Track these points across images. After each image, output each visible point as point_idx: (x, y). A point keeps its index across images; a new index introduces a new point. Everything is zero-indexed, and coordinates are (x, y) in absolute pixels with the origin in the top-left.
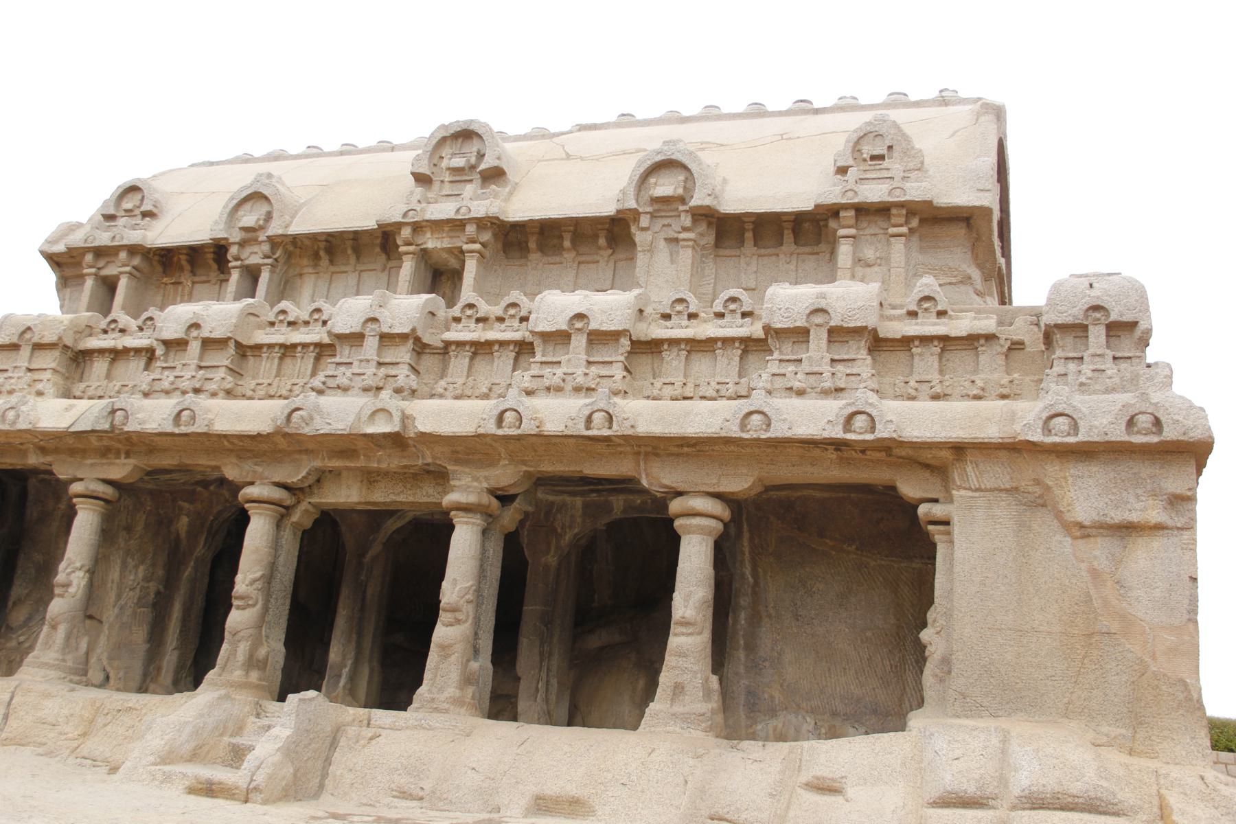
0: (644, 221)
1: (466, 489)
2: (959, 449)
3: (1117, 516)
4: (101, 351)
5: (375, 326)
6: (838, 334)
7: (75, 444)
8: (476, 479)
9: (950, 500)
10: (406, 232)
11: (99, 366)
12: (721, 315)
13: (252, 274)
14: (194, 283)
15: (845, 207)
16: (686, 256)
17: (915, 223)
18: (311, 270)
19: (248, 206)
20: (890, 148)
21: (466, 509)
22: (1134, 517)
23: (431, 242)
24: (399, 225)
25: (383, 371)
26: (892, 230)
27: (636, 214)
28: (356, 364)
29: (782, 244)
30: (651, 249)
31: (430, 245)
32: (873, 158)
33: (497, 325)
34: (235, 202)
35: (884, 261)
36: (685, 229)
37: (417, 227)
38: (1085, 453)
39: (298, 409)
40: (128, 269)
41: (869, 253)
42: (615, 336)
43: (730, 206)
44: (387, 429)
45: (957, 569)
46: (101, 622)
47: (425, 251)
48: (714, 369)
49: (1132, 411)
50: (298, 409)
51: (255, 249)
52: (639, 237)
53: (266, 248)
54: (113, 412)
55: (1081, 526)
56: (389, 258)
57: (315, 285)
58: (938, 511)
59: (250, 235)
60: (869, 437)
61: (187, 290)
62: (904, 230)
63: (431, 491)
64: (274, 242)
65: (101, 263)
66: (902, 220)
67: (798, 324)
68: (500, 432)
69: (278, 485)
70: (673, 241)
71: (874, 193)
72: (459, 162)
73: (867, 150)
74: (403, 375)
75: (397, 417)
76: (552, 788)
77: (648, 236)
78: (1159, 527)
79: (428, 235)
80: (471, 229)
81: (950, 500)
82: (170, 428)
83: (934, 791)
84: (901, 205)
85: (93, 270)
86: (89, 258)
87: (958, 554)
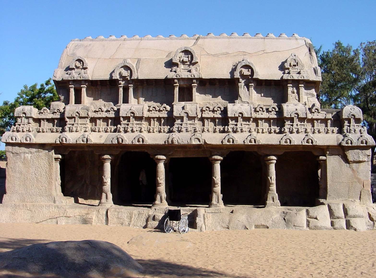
3: (358, 159)
13: (126, 90)
16: (252, 89)
17: (304, 83)
20: (297, 63)
26: (300, 85)
28: (183, 124)
33: (215, 112)
37: (178, 79)
39: (174, 138)
50: (174, 138)
55: (351, 161)
57: (143, 90)
62: (303, 85)
71: (296, 77)
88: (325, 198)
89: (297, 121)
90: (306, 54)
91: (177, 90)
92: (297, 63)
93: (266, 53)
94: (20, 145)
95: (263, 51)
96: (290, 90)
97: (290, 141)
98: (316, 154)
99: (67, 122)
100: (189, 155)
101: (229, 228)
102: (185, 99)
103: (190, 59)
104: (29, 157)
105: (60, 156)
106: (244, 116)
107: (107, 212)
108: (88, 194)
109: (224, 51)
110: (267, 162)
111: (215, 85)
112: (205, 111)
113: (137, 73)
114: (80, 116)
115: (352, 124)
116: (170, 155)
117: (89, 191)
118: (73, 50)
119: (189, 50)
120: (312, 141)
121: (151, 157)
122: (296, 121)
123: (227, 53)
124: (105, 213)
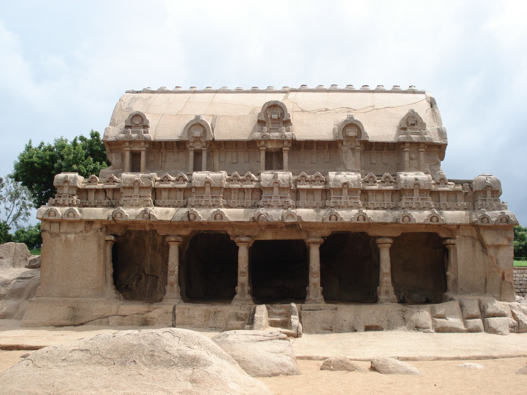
0: (345, 143)
1: (315, 237)
2: (458, 226)
3: (497, 243)
4: (165, 189)
5: (277, 185)
6: (421, 191)
7: (169, 225)
8: (317, 233)
9: (454, 238)
10: (263, 143)
11: (165, 194)
12: (383, 182)
13: (198, 154)
14: (166, 152)
15: (407, 143)
16: (358, 154)
17: (426, 147)
18: (217, 150)
19: (194, 128)
20: (416, 121)
21: (315, 243)
22: (501, 243)
23: (270, 146)
24: (260, 141)
25: (283, 200)
26: (421, 150)
27: (342, 142)
29: (383, 150)
30: (346, 152)
31: (270, 147)
32: (412, 124)
33: (313, 183)
34: (190, 126)
35: (418, 158)
36: (357, 146)
38: (490, 228)
40: (145, 149)
41: (413, 156)
42: (356, 190)
43: (370, 139)
44: (293, 221)
45: (458, 257)
46: (158, 277)
47: (267, 149)
48: (384, 197)
49: (502, 217)
51: (199, 143)
52: (344, 148)
53: (204, 144)
54: (188, 216)
56: (248, 148)
57: (220, 156)
58: (452, 241)
59: (197, 139)
60: (436, 223)
61: (164, 154)
62: (423, 150)
63: (296, 235)
64: (207, 142)
65: (131, 146)
66: (423, 147)
67: (411, 188)
68: (331, 222)
69: (248, 236)
70: (353, 149)
72: (275, 116)
73: (410, 122)
74: (291, 202)
75: (296, 218)
76: (370, 323)
77: (346, 148)
78: (506, 246)
79: (269, 144)
80: (286, 143)
81: (454, 238)
82: (214, 221)
83: (465, 316)
84: (423, 143)
85: (129, 149)
86: (127, 144)
87: (458, 253)
88: (456, 292)
89: (418, 194)
90: (427, 111)
91: (263, 155)
92: (416, 121)
93: (376, 109)
94: (60, 222)
95: (373, 106)
96: (407, 156)
97: (410, 220)
98: (443, 235)
99: (122, 193)
100: (279, 237)
101: (332, 330)
102: (274, 168)
103: (280, 116)
104: (72, 239)
105: (112, 238)
106: (350, 187)
107: (174, 309)
108: (148, 289)
109: (323, 107)
110: (379, 246)
111: (312, 148)
112: (300, 181)
113: (213, 133)
114: (141, 185)
115: (488, 198)
116: (255, 237)
117: (149, 285)
118: (129, 104)
119: (279, 104)
120: (437, 218)
121: (231, 239)
122: (416, 194)
123: (327, 110)
124: (171, 310)
